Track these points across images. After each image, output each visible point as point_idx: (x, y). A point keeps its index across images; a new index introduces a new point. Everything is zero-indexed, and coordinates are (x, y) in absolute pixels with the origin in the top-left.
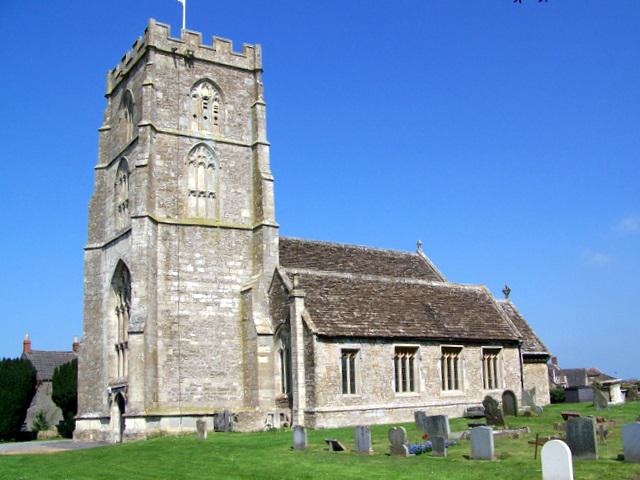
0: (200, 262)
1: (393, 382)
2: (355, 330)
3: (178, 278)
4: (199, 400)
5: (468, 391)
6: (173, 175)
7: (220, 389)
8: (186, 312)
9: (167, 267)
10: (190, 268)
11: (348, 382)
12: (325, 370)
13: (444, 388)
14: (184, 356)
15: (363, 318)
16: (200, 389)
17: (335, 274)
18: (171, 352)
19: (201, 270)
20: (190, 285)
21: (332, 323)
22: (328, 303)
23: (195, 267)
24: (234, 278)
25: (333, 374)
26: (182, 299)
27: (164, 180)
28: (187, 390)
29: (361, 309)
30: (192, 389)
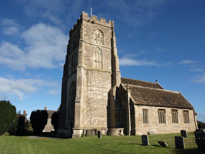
0: (97, 82)
1: (158, 120)
2: (146, 103)
3: (91, 86)
4: (97, 124)
5: (180, 124)
6: (89, 56)
7: (103, 121)
8: (93, 97)
9: (87, 82)
10: (94, 83)
11: (145, 119)
12: (138, 116)
13: (173, 123)
14: (92, 110)
15: (147, 99)
16: (97, 121)
17: (138, 86)
18: (88, 109)
19: (98, 84)
20: (94, 88)
21: (139, 100)
22: (137, 95)
23: (96, 83)
24: (107, 87)
25: (140, 117)
26: (92, 93)
27: (87, 57)
28: (93, 121)
29: (147, 97)
30: (95, 121)
